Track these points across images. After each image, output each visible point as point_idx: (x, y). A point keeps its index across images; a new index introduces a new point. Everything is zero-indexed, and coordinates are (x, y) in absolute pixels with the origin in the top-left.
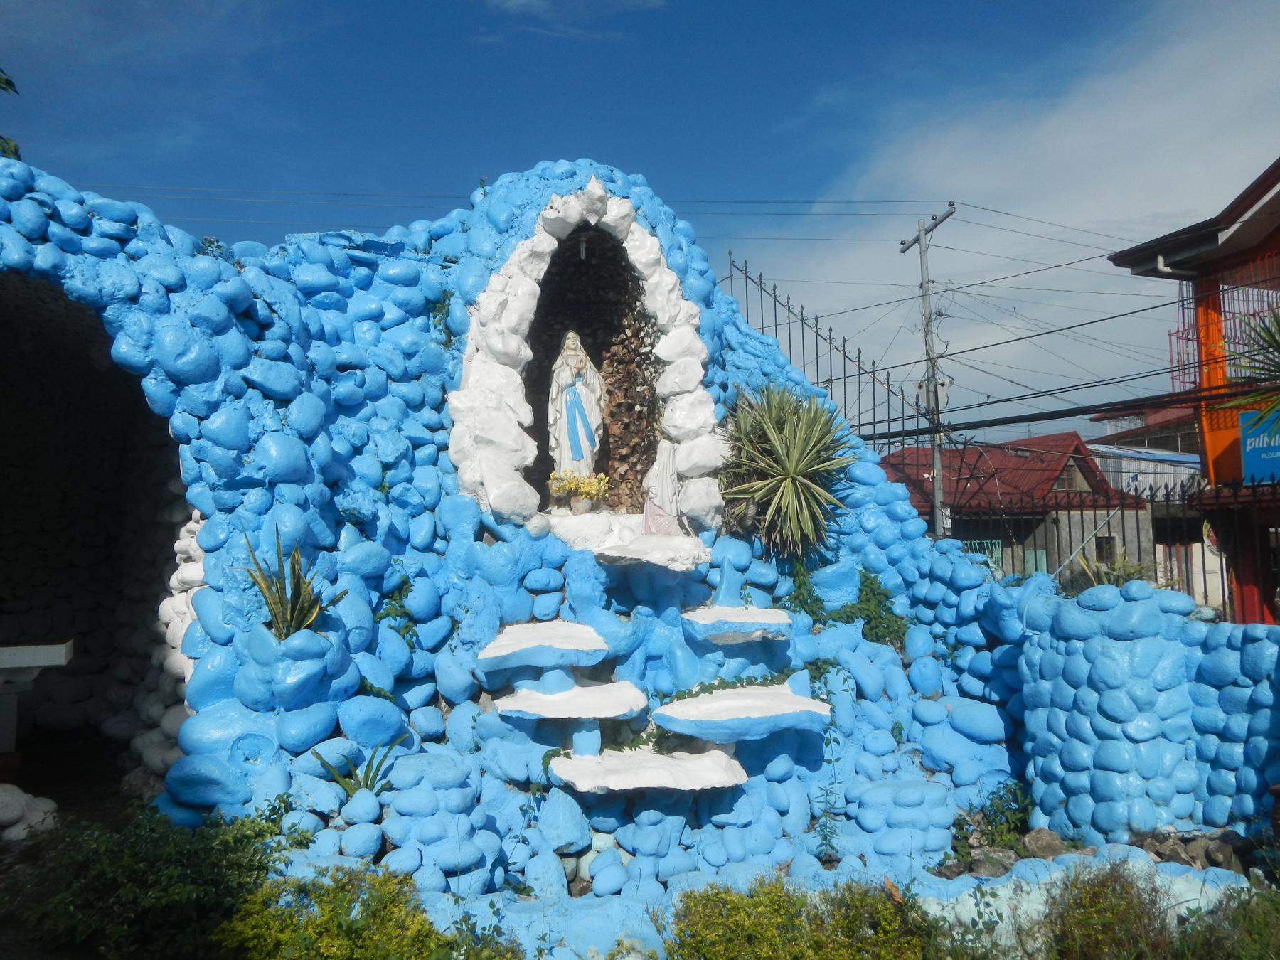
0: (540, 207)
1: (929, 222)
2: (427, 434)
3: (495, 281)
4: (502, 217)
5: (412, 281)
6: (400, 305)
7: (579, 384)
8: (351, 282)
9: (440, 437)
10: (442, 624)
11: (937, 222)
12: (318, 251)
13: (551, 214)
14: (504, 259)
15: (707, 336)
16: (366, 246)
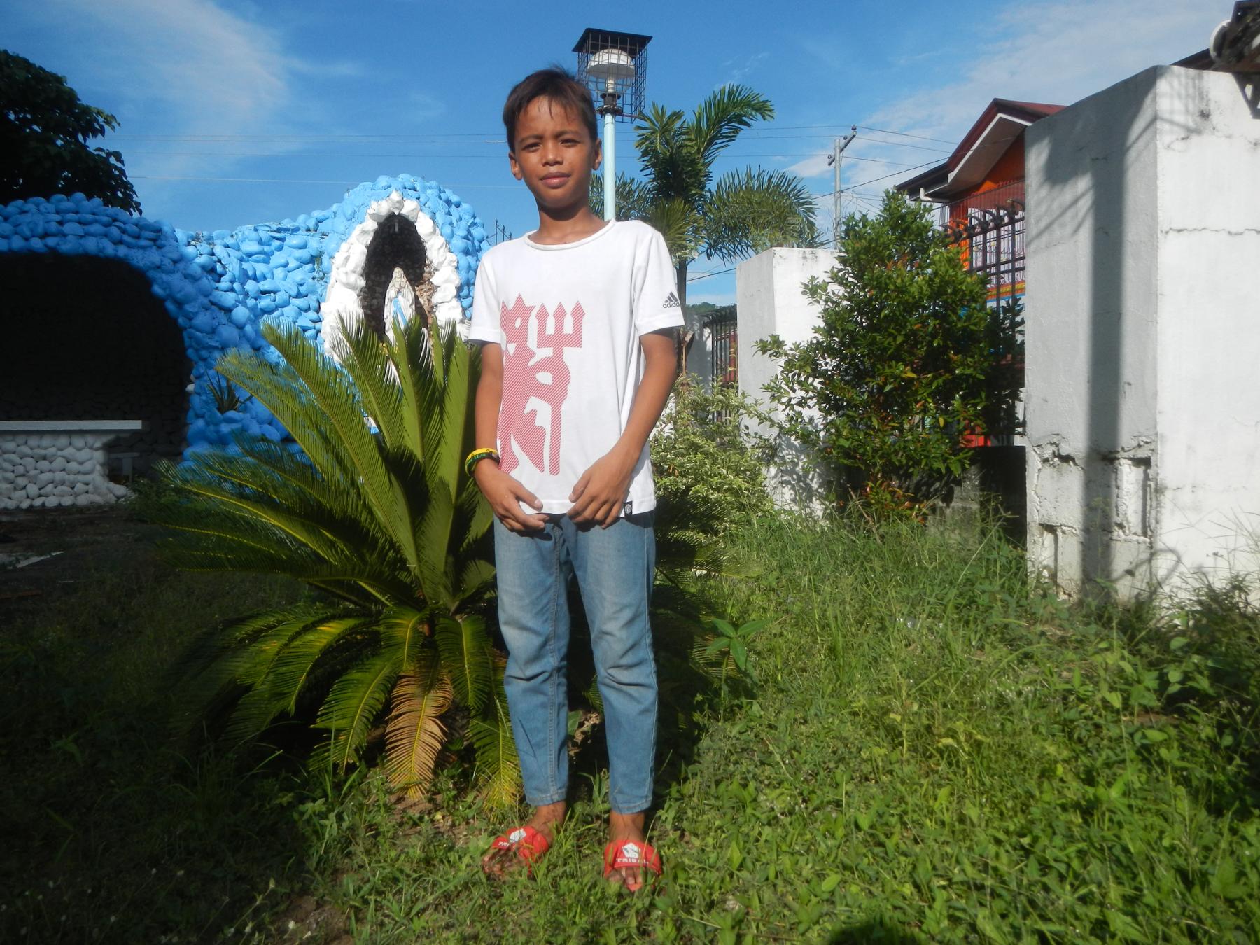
0: (368, 206)
1: (843, 142)
2: (311, 325)
3: (344, 246)
4: (349, 213)
5: (304, 247)
6: (297, 259)
7: (400, 297)
8: (273, 248)
9: (318, 326)
11: (848, 140)
12: (254, 234)
13: (371, 211)
14: (350, 234)
15: (463, 273)
16: (279, 230)
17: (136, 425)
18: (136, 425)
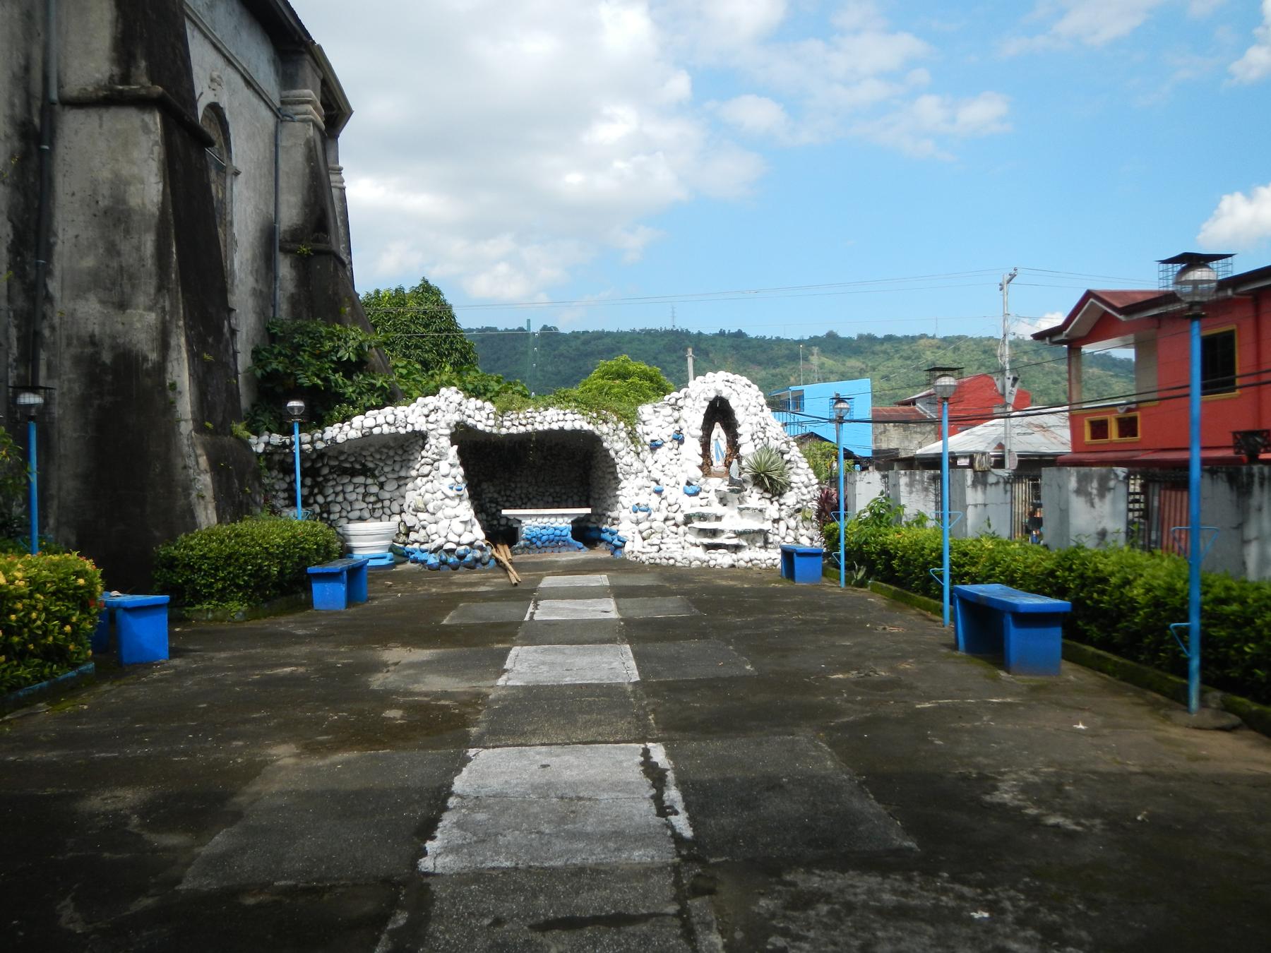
2: (675, 457)
9: (678, 457)
10: (677, 506)
11: (1013, 276)
17: (588, 511)
18: (588, 511)
